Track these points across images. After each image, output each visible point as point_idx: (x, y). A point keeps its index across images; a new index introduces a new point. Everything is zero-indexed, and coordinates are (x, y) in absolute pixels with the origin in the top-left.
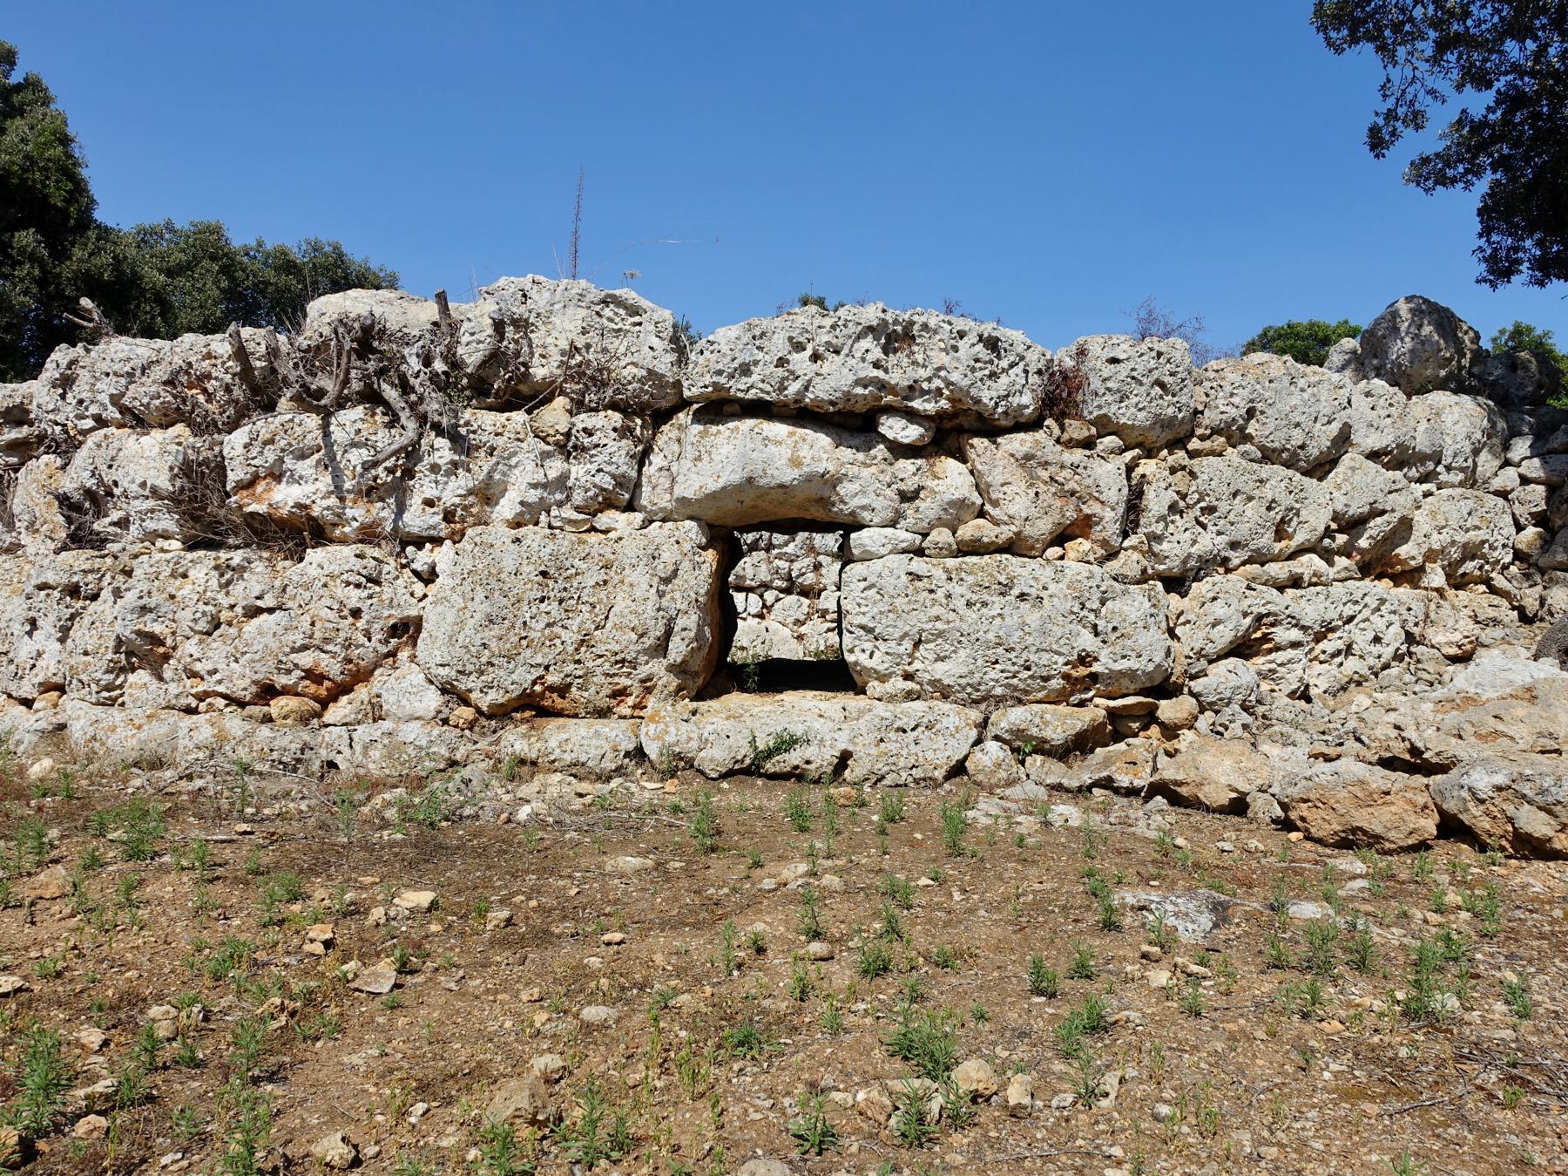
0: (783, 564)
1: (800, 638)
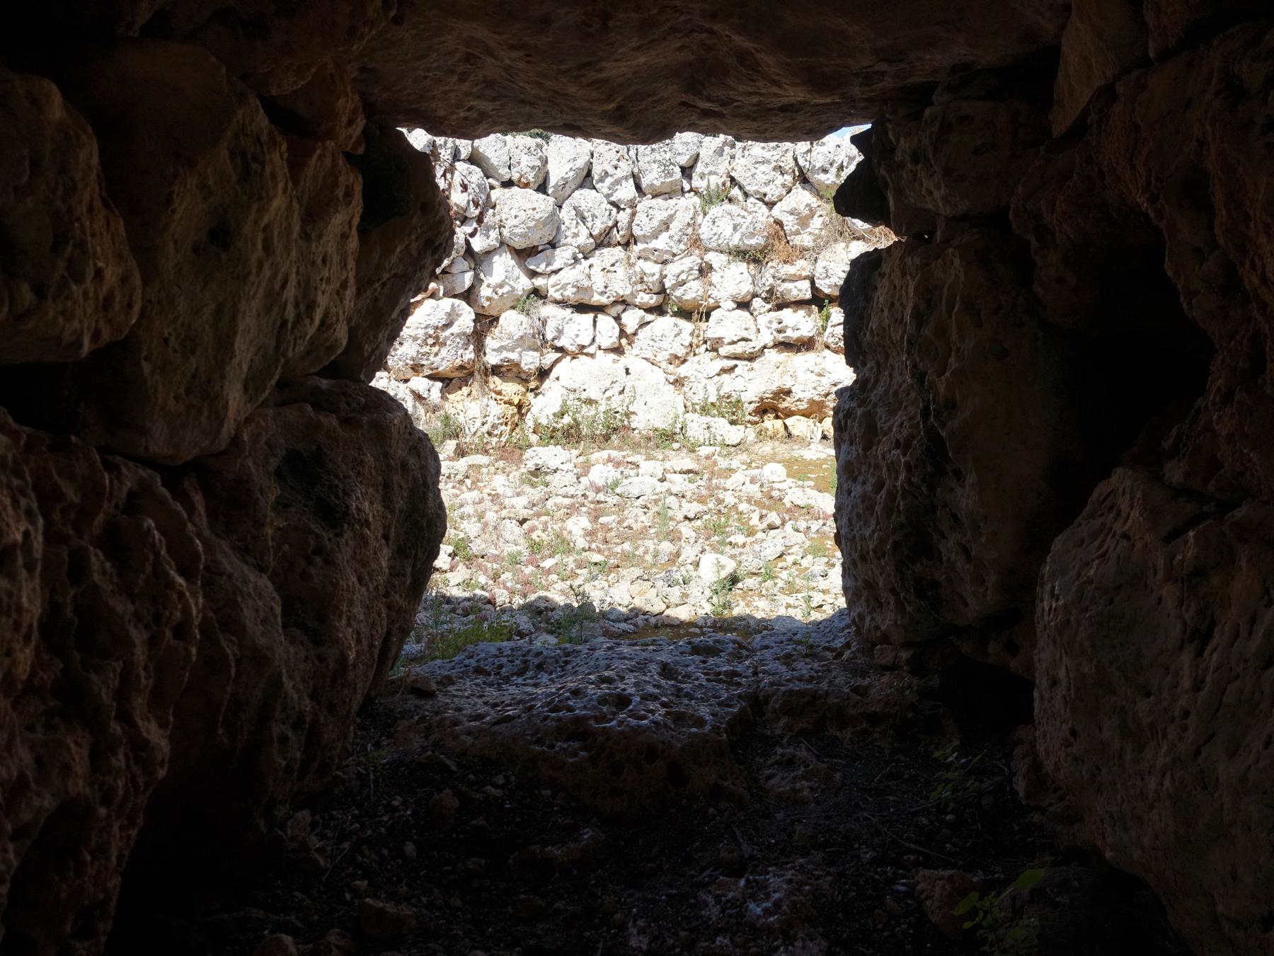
0: (651, 268)
1: (678, 382)
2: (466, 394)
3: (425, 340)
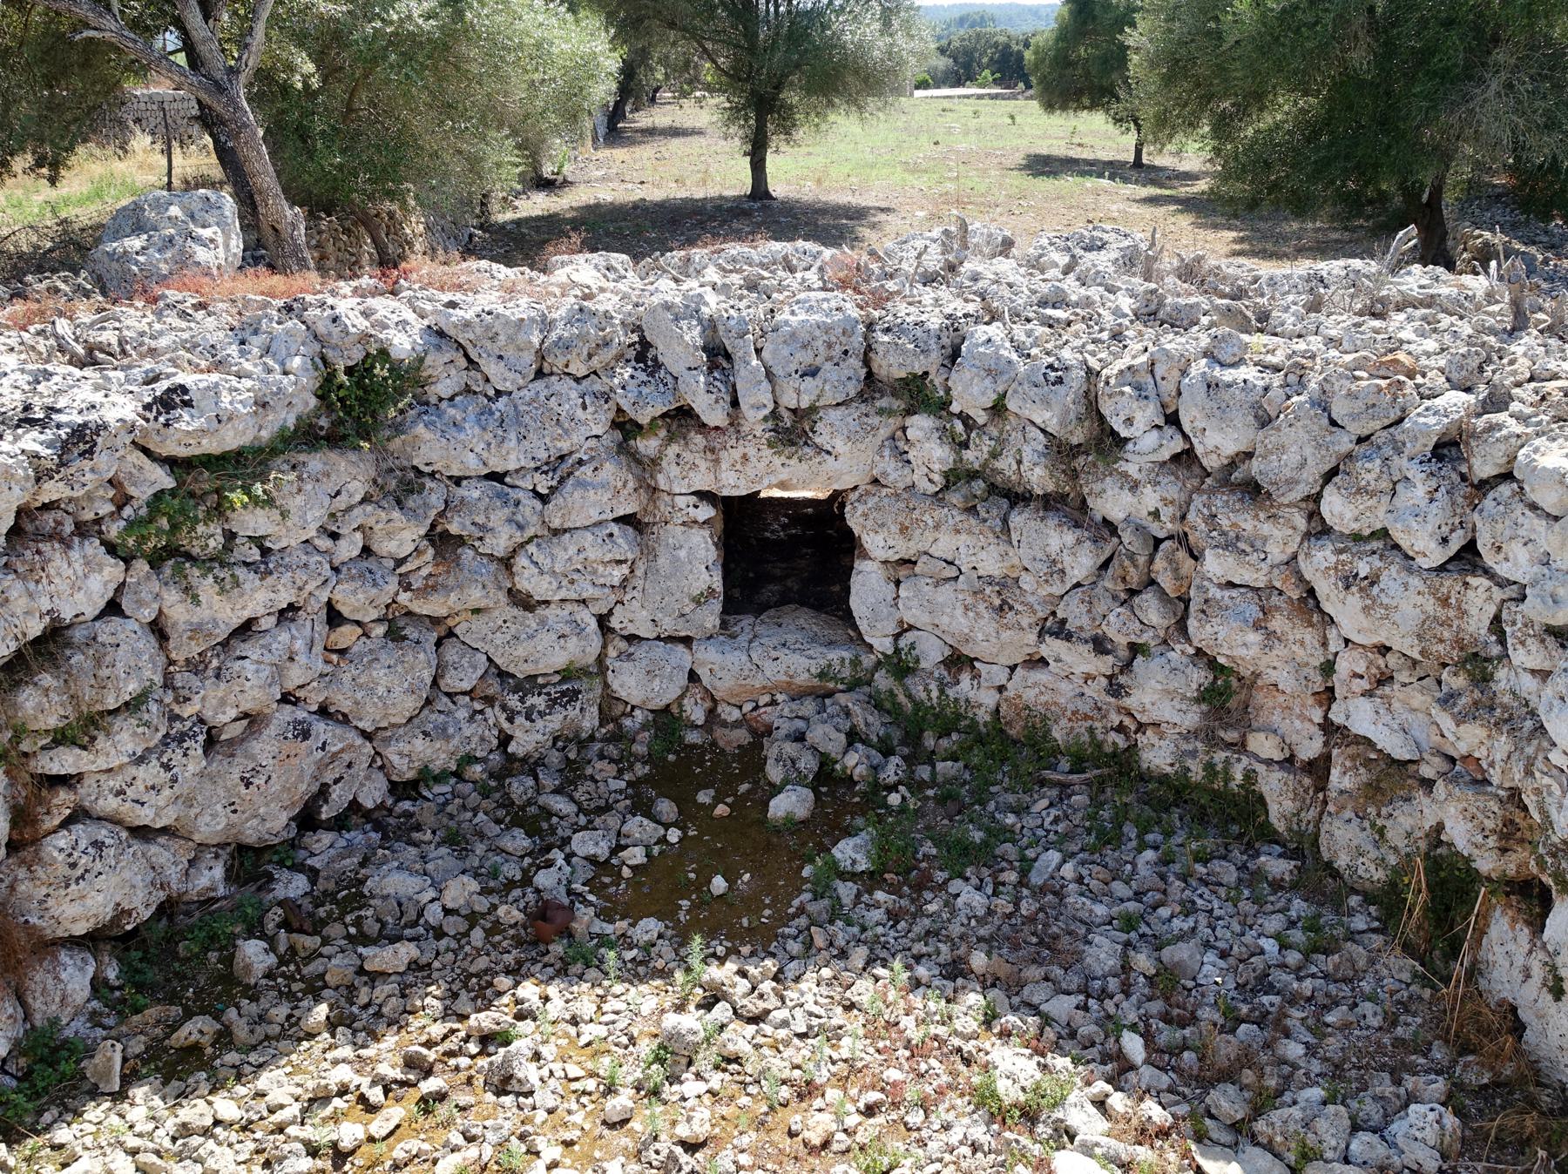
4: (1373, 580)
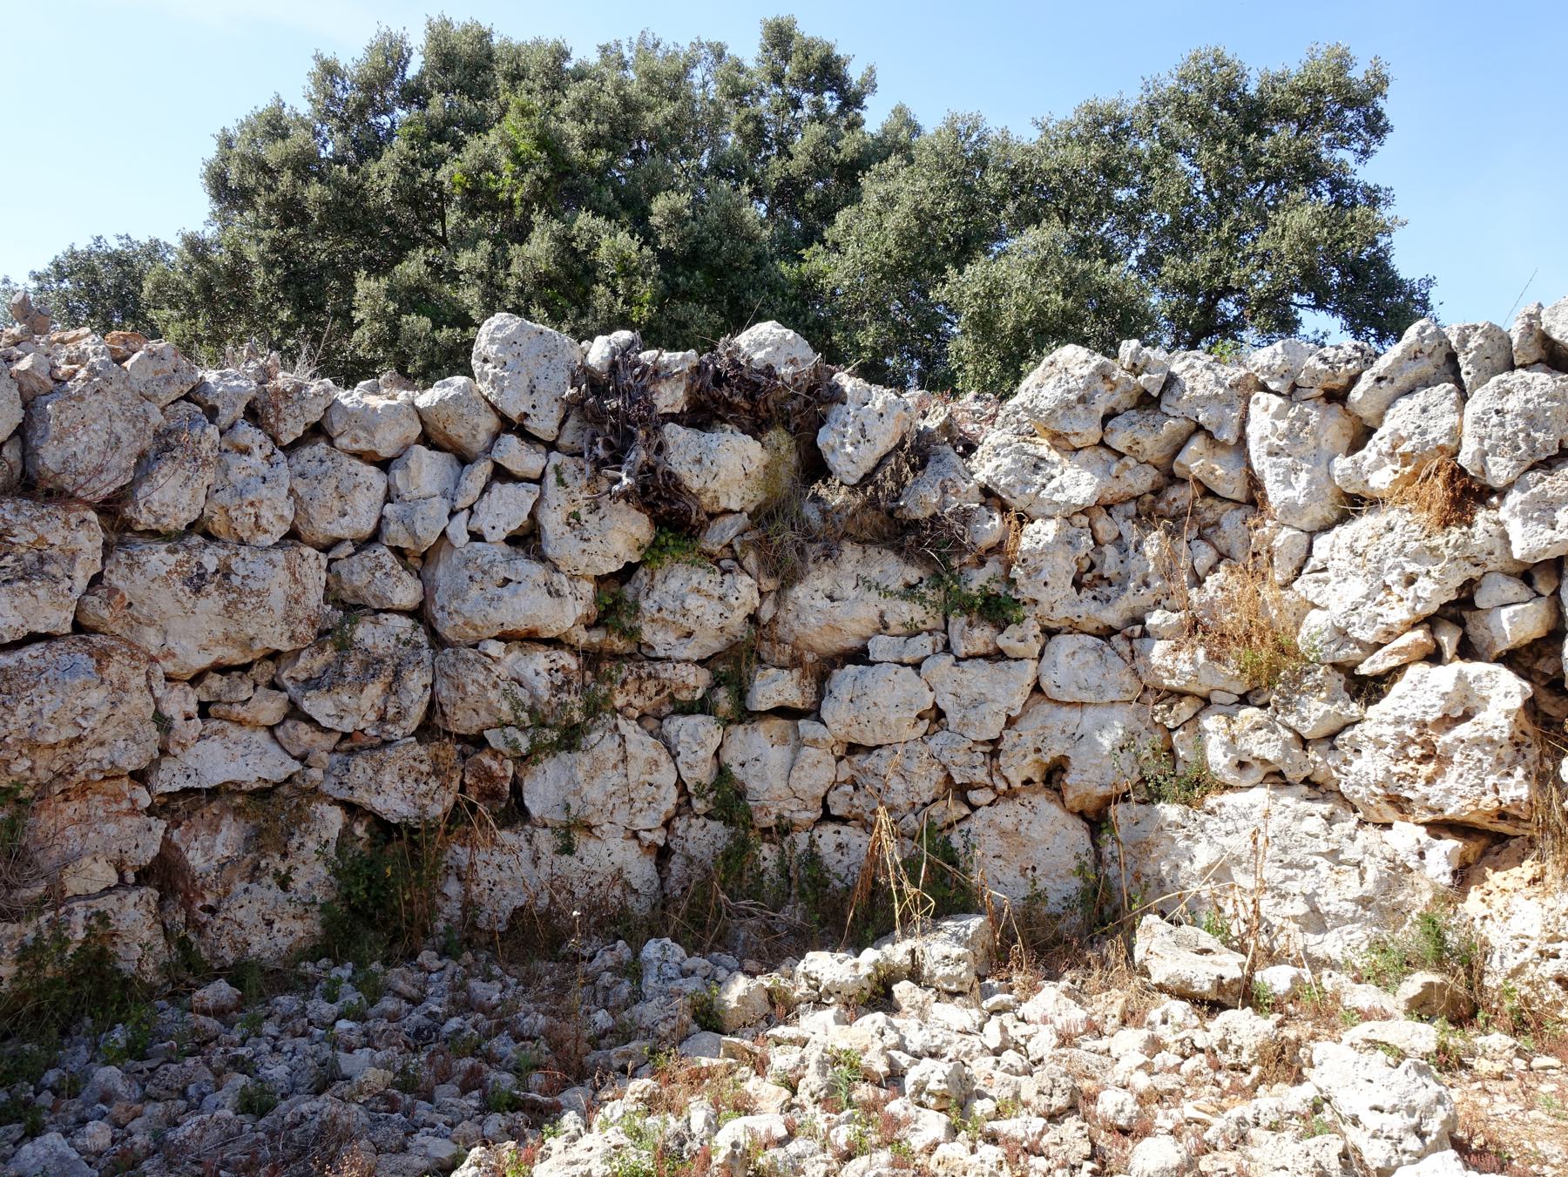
2: (1528, 877)
3: (1403, 747)
4: (225, 572)
